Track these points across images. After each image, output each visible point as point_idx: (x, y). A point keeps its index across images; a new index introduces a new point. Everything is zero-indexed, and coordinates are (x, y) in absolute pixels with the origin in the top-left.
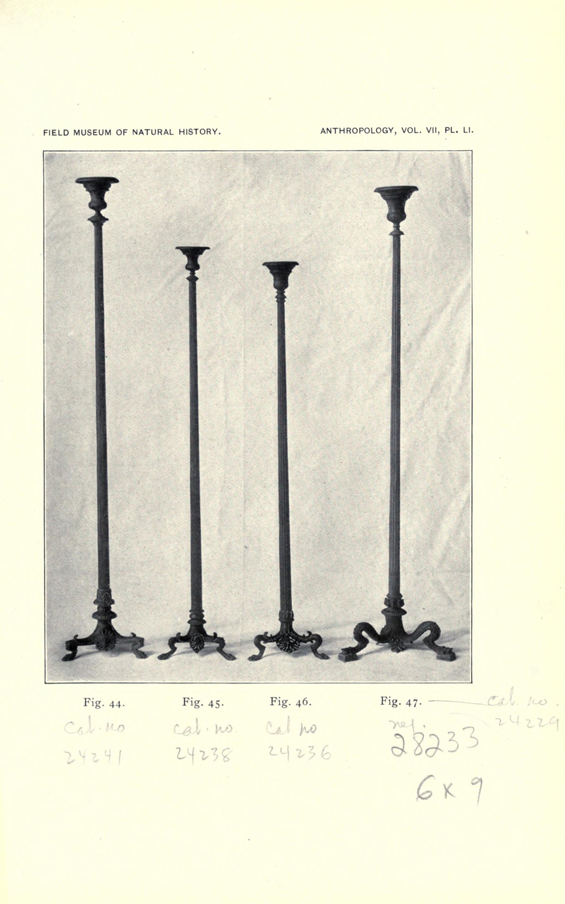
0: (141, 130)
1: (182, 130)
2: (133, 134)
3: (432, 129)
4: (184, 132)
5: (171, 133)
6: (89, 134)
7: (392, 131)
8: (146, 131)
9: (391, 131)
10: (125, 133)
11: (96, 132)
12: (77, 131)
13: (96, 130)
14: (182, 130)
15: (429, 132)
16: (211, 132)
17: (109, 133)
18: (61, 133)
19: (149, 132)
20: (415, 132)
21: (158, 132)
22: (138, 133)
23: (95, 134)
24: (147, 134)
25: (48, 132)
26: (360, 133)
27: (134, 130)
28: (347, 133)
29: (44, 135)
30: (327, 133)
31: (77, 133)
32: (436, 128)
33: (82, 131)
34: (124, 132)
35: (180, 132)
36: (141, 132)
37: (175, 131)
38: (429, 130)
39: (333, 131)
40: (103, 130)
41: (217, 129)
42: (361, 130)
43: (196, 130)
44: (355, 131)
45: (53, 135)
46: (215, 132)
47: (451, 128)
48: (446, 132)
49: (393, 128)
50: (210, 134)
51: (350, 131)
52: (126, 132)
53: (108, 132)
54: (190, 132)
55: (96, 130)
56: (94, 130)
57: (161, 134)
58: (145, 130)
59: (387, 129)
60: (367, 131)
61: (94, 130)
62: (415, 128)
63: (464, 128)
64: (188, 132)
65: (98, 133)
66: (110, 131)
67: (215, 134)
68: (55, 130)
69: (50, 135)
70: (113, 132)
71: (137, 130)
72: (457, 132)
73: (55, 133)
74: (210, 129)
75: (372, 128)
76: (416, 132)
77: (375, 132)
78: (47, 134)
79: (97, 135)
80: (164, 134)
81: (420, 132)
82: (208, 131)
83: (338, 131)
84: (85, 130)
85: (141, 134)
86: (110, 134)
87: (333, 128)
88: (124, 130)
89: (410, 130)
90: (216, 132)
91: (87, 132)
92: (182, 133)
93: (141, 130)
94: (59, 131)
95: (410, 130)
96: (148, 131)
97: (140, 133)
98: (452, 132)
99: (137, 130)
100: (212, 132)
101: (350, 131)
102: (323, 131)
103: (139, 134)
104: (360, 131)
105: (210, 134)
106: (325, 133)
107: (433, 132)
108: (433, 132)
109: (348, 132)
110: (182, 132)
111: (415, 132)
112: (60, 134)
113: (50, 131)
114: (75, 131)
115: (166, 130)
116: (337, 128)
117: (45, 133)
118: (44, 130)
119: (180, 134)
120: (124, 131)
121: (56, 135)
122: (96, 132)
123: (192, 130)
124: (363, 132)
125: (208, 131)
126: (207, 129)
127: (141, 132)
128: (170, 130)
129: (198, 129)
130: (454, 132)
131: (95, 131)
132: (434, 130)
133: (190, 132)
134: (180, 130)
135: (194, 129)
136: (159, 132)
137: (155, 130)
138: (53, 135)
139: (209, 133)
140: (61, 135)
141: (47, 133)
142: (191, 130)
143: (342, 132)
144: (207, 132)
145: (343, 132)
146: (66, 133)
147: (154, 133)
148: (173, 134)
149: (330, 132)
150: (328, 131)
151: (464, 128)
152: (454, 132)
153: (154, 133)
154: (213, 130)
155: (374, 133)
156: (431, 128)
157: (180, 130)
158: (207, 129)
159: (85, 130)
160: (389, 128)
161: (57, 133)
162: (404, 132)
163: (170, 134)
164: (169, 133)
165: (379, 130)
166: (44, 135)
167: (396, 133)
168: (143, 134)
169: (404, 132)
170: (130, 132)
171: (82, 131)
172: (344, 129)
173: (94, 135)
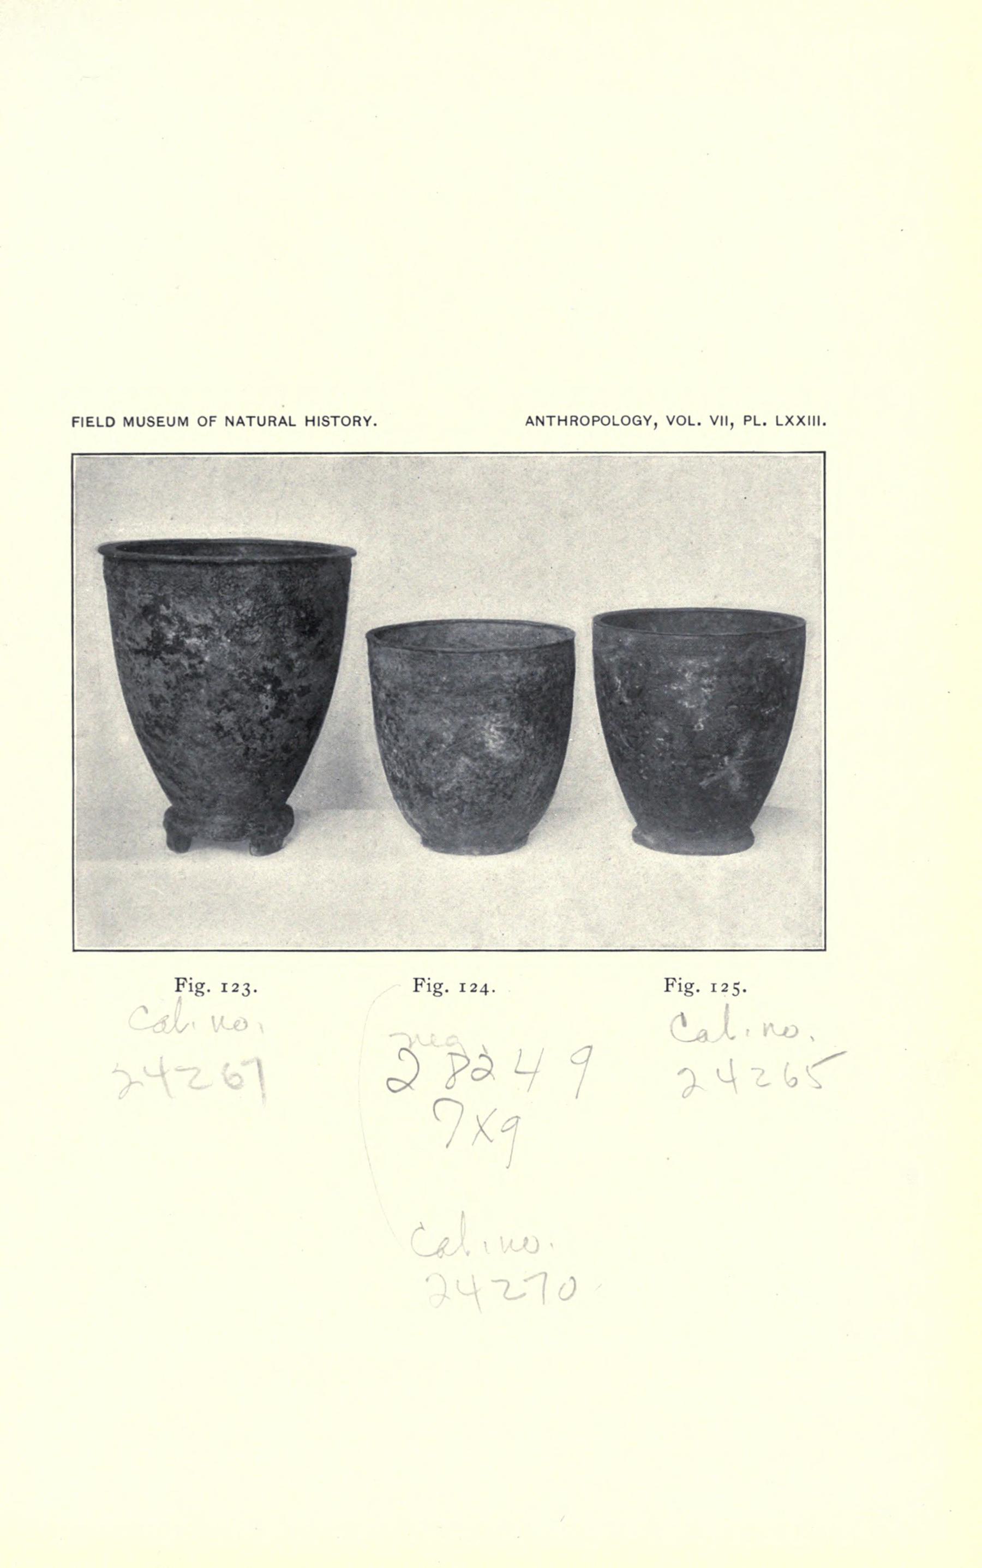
0: (240, 418)
1: (310, 418)
2: (226, 425)
3: (719, 418)
4: (313, 421)
5: (292, 423)
6: (151, 424)
7: (650, 422)
8: (249, 419)
9: (647, 421)
10: (212, 423)
11: (162, 422)
12: (129, 419)
13: (163, 417)
14: (310, 418)
15: (714, 423)
16: (361, 422)
17: (184, 422)
18: (103, 422)
19: (254, 421)
20: (690, 424)
21: (270, 421)
22: (235, 422)
23: (160, 424)
24: (251, 425)
25: (80, 420)
26: (593, 424)
27: (227, 418)
28: (571, 424)
29: (73, 426)
30: (537, 425)
31: (129, 422)
32: (727, 417)
33: (138, 418)
34: (211, 421)
35: (307, 421)
36: (240, 421)
37: (299, 420)
38: (714, 420)
39: (547, 421)
40: (174, 418)
41: (370, 417)
42: (595, 419)
43: (335, 417)
44: (585, 421)
45: (88, 426)
46: (367, 421)
47: (755, 417)
48: (745, 424)
49: (650, 417)
50: (360, 425)
51: (576, 421)
52: (214, 421)
53: (183, 419)
54: (325, 421)
55: (163, 417)
56: (158, 418)
57: (275, 425)
58: (247, 417)
59: (640, 418)
60: (605, 421)
61: (158, 418)
62: (689, 417)
63: (777, 417)
64: (321, 421)
65: (165, 423)
66: (187, 418)
67: (367, 425)
68: (92, 418)
69: (82, 426)
70: (193, 421)
71: (233, 417)
72: (765, 424)
73: (92, 422)
74: (360, 419)
75: (613, 417)
76: (691, 423)
77: (620, 423)
78: (78, 425)
79: (164, 426)
80: (279, 425)
81: (699, 424)
82: (357, 420)
83: (555, 420)
84: (144, 418)
85: (241, 425)
86: (187, 425)
87: (547, 417)
88: (211, 417)
89: (681, 420)
90: (371, 423)
91: (146, 421)
92: (310, 424)
93: (240, 418)
94: (98, 418)
95: (681, 420)
96: (253, 419)
97: (238, 423)
98: (755, 424)
99: (233, 417)
100: (363, 422)
101: (576, 421)
102: (529, 421)
103: (237, 425)
104: (594, 421)
105: (360, 425)
106: (533, 425)
107: (722, 424)
108: (722, 424)
109: (574, 423)
110: (310, 421)
111: (690, 424)
112: (100, 424)
113: (82, 419)
114: (125, 419)
115: (283, 418)
116: (554, 417)
117: (74, 422)
118: (74, 418)
119: (307, 425)
120: (212, 419)
121: (93, 426)
122: (162, 422)
123: (328, 418)
124: (598, 424)
125: (357, 420)
126: (354, 417)
127: (241, 421)
128: (290, 417)
129: (339, 417)
130: (759, 425)
131: (160, 419)
132: (724, 420)
133: (325, 421)
134: (306, 417)
135: (332, 417)
136: (272, 420)
137: (265, 417)
138: (88, 426)
139: (357, 423)
140: (102, 426)
141: (77, 422)
142: (326, 419)
143: (563, 423)
144: (354, 421)
145: (564, 422)
146: (110, 422)
147: (261, 423)
148: (295, 425)
149: (543, 423)
150: (539, 421)
151: (777, 417)
152: (759, 425)
153: (261, 423)
154: (364, 418)
155: (618, 425)
156: (718, 417)
157: (306, 417)
158: (354, 417)
159: (144, 418)
160: (644, 417)
161: (95, 423)
162: (671, 423)
163: (290, 425)
165: (626, 420)
166: (73, 426)
167: (656, 424)
168: (244, 425)
169: (671, 423)
170: (220, 420)
171: (138, 418)
172: (566, 417)
173: (158, 425)
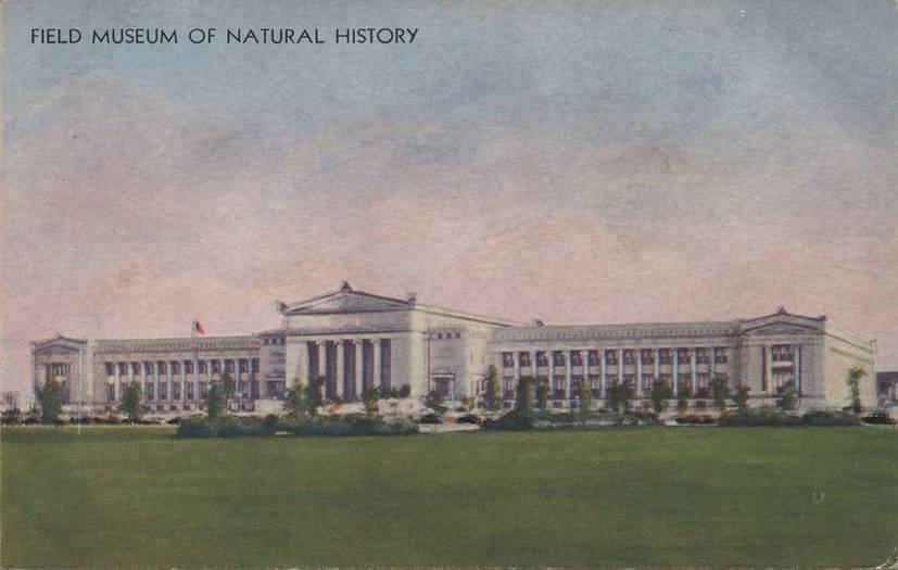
12: (101, 34)
18: (64, 37)
22: (242, 40)
34: (210, 36)
35: (338, 36)
45: (48, 42)
82: (397, 35)
100: (407, 37)
134: (337, 31)
138: (48, 42)
142: (361, 32)
154: (408, 30)
157: (337, 31)
161: (55, 39)
164: (314, 39)
